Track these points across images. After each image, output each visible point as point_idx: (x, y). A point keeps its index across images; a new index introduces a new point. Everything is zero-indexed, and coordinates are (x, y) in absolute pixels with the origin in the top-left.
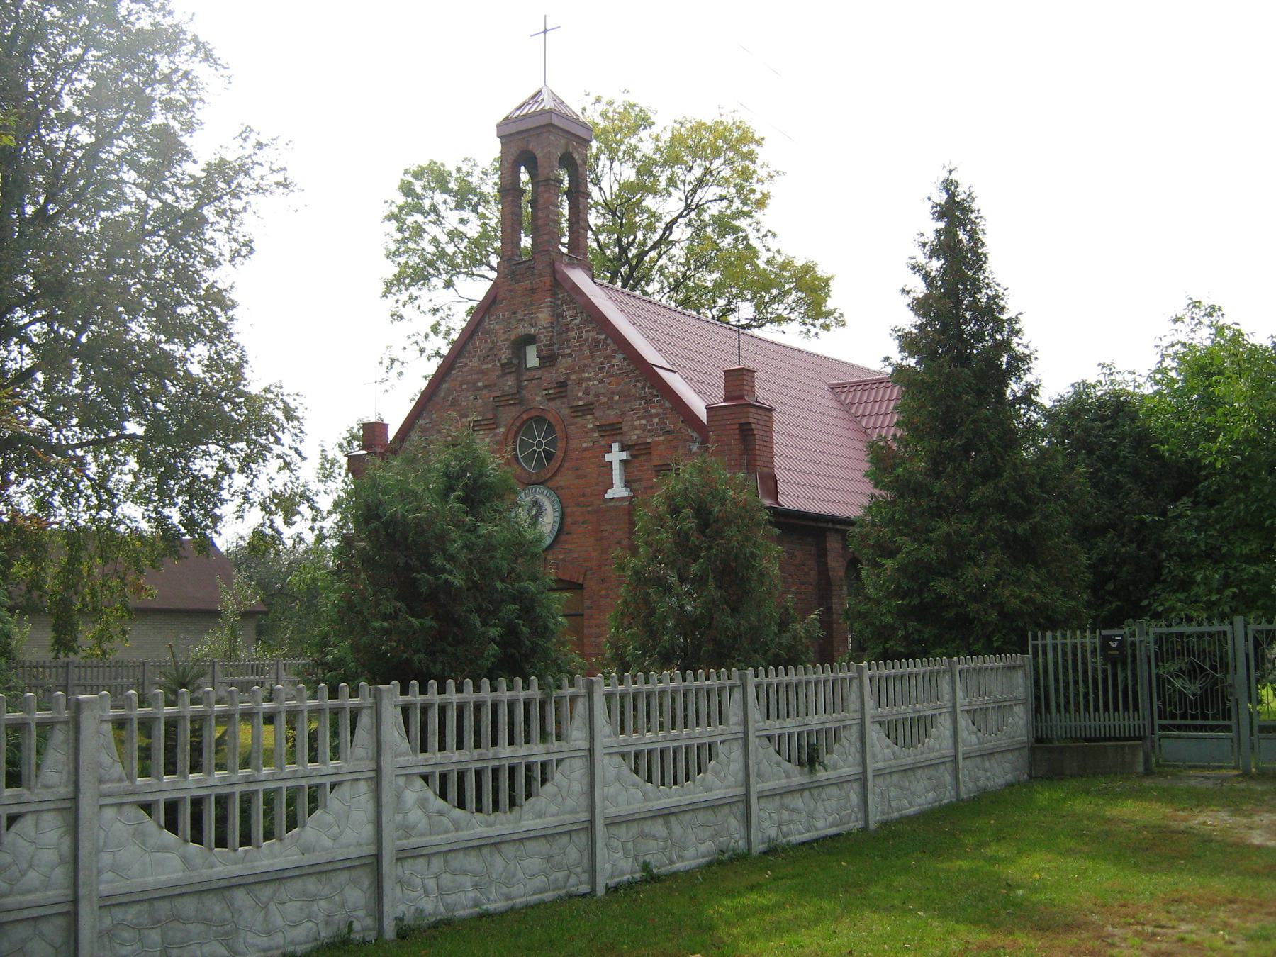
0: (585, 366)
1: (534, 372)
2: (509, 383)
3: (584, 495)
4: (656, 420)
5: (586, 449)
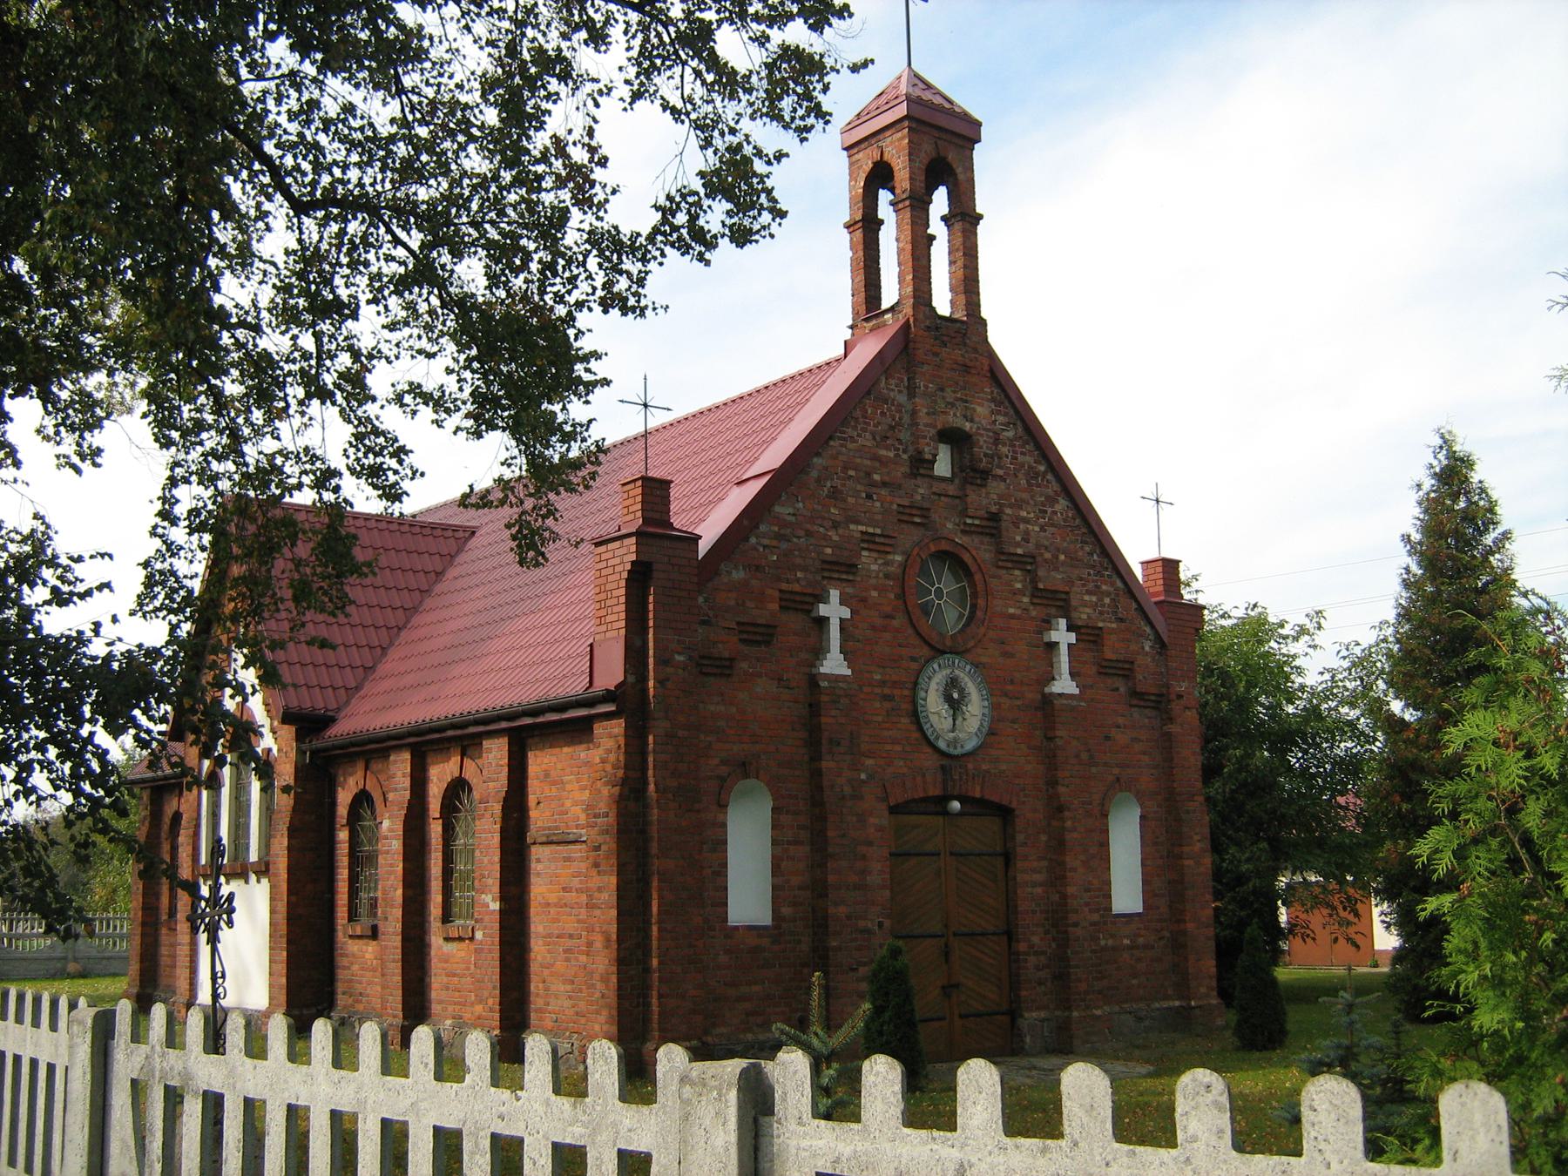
0: (1023, 500)
1: (943, 485)
2: (921, 491)
3: (1012, 682)
4: (1107, 600)
5: (1012, 616)
